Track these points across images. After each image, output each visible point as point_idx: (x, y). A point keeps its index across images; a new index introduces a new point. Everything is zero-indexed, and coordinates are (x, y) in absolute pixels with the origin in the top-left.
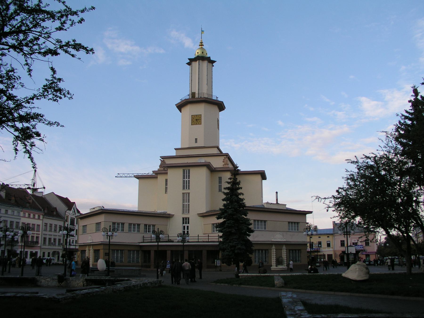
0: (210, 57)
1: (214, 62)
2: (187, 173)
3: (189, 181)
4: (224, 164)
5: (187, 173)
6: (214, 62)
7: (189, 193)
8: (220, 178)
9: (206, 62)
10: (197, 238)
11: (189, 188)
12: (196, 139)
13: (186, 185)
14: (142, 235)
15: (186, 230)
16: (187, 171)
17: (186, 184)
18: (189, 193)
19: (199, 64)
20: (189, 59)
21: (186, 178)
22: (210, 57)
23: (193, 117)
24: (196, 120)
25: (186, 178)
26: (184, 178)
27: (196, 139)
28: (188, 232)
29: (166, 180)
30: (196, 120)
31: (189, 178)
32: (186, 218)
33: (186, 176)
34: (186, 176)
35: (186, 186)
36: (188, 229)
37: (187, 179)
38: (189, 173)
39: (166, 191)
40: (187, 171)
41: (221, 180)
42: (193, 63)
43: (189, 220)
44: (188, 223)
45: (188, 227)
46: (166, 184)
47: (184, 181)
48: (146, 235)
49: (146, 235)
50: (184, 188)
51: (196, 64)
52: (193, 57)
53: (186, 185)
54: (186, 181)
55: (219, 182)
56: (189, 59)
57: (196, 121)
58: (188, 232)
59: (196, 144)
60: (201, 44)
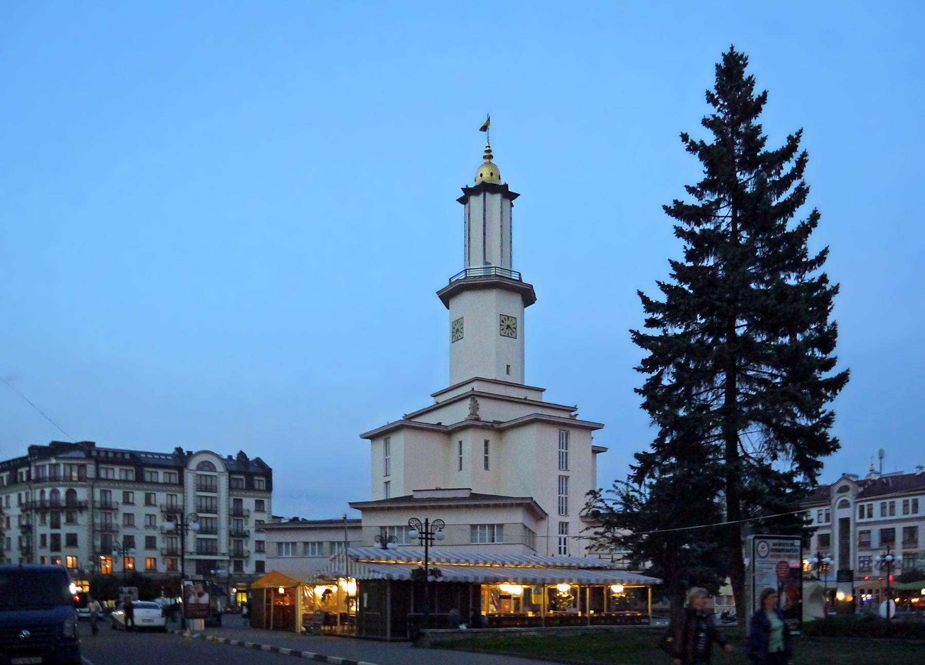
7: (567, 478)
12: (508, 367)
13: (563, 461)
15: (562, 546)
18: (567, 478)
24: (508, 327)
27: (508, 367)
28: (565, 548)
32: (563, 523)
33: (564, 443)
37: (564, 451)
39: (486, 467)
45: (565, 539)
52: (472, 185)
57: (505, 327)
58: (565, 548)
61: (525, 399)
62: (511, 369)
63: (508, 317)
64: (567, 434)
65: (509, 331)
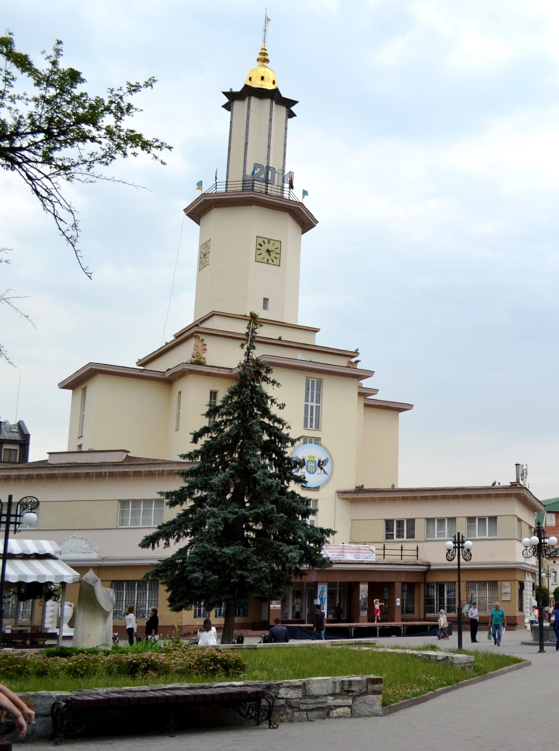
2: (313, 389)
3: (318, 408)
5: (313, 389)
11: (318, 427)
12: (266, 300)
16: (313, 382)
17: (312, 415)
21: (312, 401)
24: (268, 251)
25: (312, 401)
26: (307, 400)
27: (266, 300)
31: (318, 401)
37: (314, 404)
38: (319, 388)
40: (313, 382)
47: (306, 406)
50: (306, 426)
54: (312, 407)
59: (264, 311)
61: (280, 339)
62: (270, 304)
64: (320, 383)
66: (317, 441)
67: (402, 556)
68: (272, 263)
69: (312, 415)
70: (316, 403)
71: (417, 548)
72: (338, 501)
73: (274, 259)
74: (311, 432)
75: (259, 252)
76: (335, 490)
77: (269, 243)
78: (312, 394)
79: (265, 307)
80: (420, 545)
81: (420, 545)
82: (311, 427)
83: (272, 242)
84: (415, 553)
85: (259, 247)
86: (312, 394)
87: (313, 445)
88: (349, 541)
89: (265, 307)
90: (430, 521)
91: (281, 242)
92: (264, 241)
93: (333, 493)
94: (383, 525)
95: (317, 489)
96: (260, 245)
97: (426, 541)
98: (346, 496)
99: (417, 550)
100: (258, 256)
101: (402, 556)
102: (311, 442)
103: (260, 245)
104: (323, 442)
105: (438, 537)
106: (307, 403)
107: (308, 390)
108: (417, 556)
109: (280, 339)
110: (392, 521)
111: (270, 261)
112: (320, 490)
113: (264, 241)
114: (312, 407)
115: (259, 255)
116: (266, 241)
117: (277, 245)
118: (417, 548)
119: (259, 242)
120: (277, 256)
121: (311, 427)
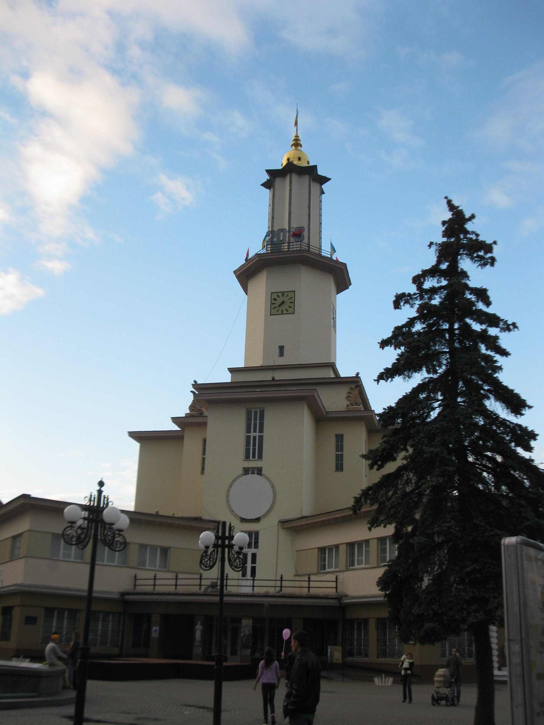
0: (315, 167)
1: (324, 180)
2: (255, 419)
3: (261, 438)
4: (348, 403)
5: (255, 419)
6: (324, 180)
8: (339, 438)
9: (306, 179)
10: (278, 584)
11: (260, 457)
12: (281, 348)
14: (133, 572)
16: (256, 413)
17: (254, 445)
19: (291, 182)
20: (269, 172)
22: (315, 167)
23: (275, 296)
24: (283, 302)
26: (248, 431)
27: (281, 348)
28: (253, 570)
29: (205, 441)
30: (281, 304)
31: (261, 431)
33: (255, 423)
34: (255, 423)
35: (254, 450)
36: (254, 561)
37: (257, 434)
40: (256, 413)
41: (342, 441)
42: (278, 182)
43: (257, 538)
44: (256, 546)
45: (254, 556)
46: (204, 453)
47: (248, 438)
48: (141, 574)
49: (141, 574)
50: (247, 457)
51: (283, 185)
53: (254, 448)
54: (255, 438)
55: (337, 446)
56: (269, 172)
58: (253, 570)
60: (297, 144)
61: (273, 379)
63: (283, 293)
65: (283, 307)
66: (259, 471)
67: (309, 588)
68: (287, 313)
69: (254, 445)
70: (259, 432)
71: (337, 579)
72: (281, 530)
73: (288, 309)
74: (254, 462)
75: (273, 306)
76: (278, 520)
77: (283, 296)
78: (255, 425)
79: (281, 354)
80: (341, 576)
81: (341, 576)
82: (254, 456)
83: (286, 294)
84: (334, 585)
85: (273, 302)
86: (255, 425)
87: (256, 476)
88: (294, 573)
89: (281, 354)
90: (351, 545)
91: (294, 291)
92: (278, 296)
93: (276, 522)
94: (315, 556)
95: (258, 520)
96: (275, 299)
97: (347, 570)
98: (287, 525)
99: (336, 582)
100: (273, 310)
101: (309, 588)
102: (253, 473)
103: (275, 299)
104: (264, 472)
105: (358, 565)
106: (249, 434)
107: (251, 420)
108: (336, 588)
109: (273, 379)
110: (254, 548)
111: (285, 312)
112: (261, 522)
113: (278, 296)
114: (255, 438)
115: (274, 308)
116: (280, 294)
117: (291, 295)
118: (337, 579)
119: (273, 298)
120: (292, 305)
121: (254, 456)
